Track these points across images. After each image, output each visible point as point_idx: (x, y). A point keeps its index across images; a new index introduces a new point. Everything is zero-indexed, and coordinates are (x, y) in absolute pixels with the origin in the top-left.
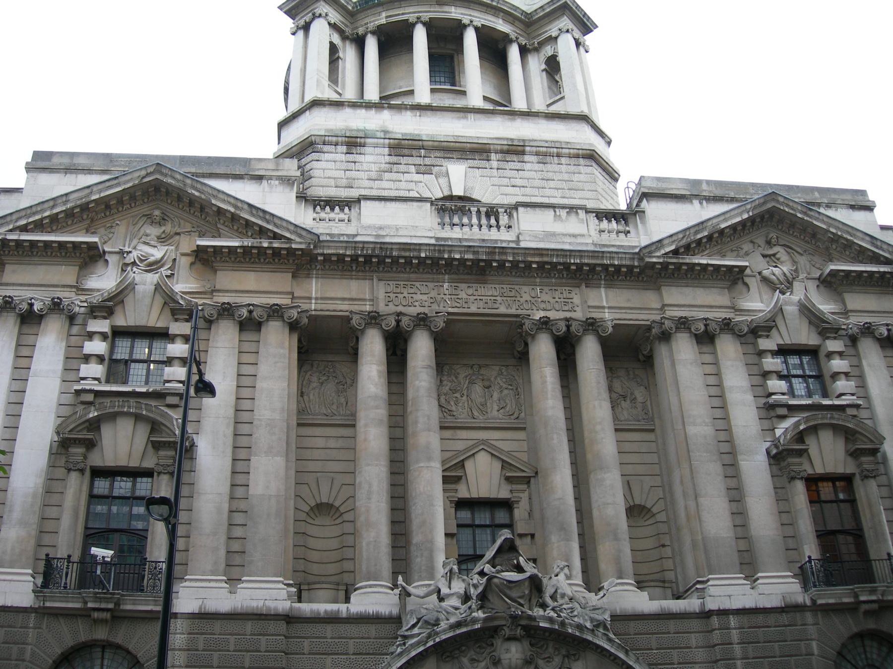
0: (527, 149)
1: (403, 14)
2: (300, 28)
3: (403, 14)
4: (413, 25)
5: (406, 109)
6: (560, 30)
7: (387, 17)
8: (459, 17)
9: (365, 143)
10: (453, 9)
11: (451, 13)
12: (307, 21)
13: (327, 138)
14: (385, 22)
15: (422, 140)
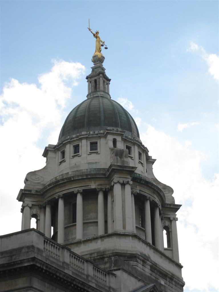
0: (174, 279)
1: (145, 192)
2: (119, 183)
3: (145, 192)
4: (147, 200)
5: (152, 248)
6: (174, 218)
7: (140, 190)
8: (158, 202)
9: (146, 262)
10: (155, 196)
11: (155, 198)
12: (125, 182)
13: (140, 257)
14: (139, 192)
15: (157, 267)
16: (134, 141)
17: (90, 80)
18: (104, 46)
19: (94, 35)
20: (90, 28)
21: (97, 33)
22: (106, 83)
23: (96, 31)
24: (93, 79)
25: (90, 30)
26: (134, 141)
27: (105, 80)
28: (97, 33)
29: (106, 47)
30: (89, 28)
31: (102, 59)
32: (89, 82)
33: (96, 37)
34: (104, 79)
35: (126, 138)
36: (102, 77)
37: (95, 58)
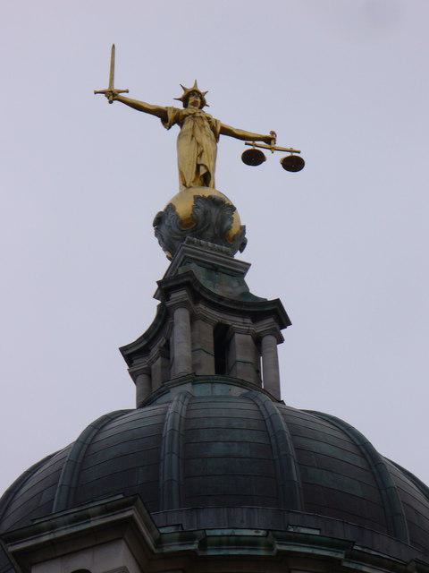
16: (270, 547)
17: (141, 363)
18: (273, 159)
19: (161, 114)
20: (117, 87)
21: (192, 99)
22: (247, 333)
23: (181, 94)
24: (155, 350)
25: (112, 95)
26: (270, 547)
27: (235, 322)
28: (193, 98)
29: (294, 154)
30: (106, 87)
31: (205, 213)
32: (141, 378)
33: (179, 120)
34: (217, 316)
35: (194, 546)
36: (183, 304)
37: (164, 229)
